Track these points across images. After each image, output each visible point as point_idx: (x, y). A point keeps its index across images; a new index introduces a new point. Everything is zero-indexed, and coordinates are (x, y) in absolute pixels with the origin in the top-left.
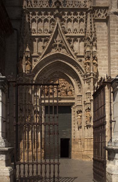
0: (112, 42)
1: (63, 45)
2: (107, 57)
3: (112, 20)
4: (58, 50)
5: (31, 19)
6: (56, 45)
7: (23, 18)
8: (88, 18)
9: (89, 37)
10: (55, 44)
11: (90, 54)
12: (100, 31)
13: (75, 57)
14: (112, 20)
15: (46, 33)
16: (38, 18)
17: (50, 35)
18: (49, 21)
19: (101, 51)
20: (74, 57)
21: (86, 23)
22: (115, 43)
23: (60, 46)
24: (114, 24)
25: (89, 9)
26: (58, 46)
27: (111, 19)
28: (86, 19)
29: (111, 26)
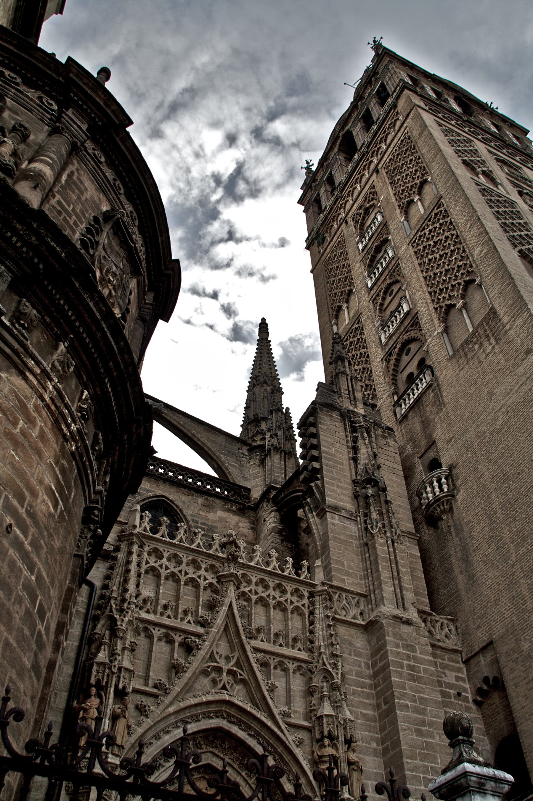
0: (399, 698)
1: (241, 675)
2: (378, 745)
3: (391, 634)
4: (224, 687)
5: (144, 567)
6: (219, 670)
7: (121, 556)
8: (317, 611)
9: (329, 668)
10: (216, 664)
11: (337, 727)
12: (350, 655)
13: (283, 726)
14: (391, 634)
15: (189, 622)
16: (168, 571)
17: (200, 630)
18: (202, 587)
19: (360, 721)
20: (279, 727)
21: (312, 623)
22: (407, 706)
23: (230, 672)
24: (397, 646)
25: (319, 588)
26: (225, 674)
27: (388, 632)
28: (312, 613)
29: (389, 652)
